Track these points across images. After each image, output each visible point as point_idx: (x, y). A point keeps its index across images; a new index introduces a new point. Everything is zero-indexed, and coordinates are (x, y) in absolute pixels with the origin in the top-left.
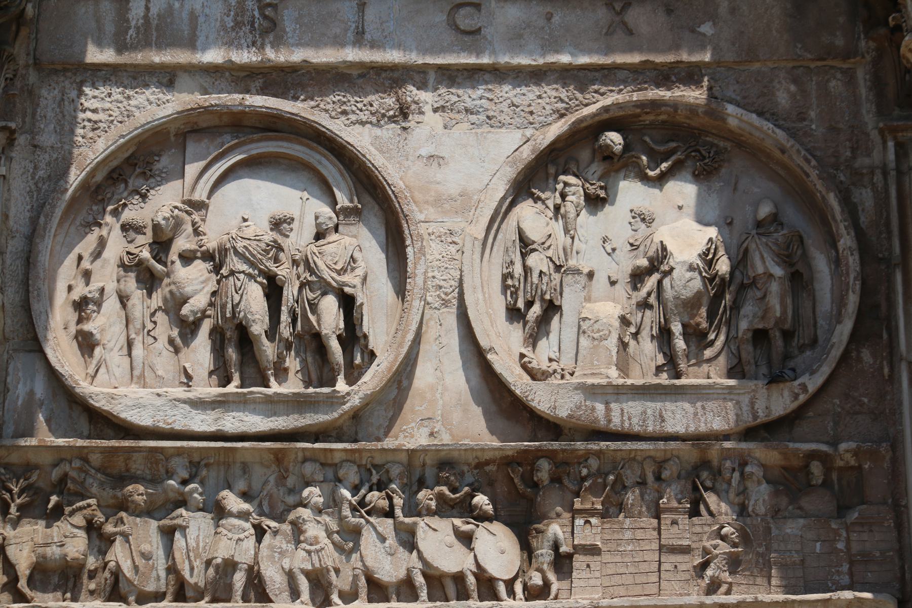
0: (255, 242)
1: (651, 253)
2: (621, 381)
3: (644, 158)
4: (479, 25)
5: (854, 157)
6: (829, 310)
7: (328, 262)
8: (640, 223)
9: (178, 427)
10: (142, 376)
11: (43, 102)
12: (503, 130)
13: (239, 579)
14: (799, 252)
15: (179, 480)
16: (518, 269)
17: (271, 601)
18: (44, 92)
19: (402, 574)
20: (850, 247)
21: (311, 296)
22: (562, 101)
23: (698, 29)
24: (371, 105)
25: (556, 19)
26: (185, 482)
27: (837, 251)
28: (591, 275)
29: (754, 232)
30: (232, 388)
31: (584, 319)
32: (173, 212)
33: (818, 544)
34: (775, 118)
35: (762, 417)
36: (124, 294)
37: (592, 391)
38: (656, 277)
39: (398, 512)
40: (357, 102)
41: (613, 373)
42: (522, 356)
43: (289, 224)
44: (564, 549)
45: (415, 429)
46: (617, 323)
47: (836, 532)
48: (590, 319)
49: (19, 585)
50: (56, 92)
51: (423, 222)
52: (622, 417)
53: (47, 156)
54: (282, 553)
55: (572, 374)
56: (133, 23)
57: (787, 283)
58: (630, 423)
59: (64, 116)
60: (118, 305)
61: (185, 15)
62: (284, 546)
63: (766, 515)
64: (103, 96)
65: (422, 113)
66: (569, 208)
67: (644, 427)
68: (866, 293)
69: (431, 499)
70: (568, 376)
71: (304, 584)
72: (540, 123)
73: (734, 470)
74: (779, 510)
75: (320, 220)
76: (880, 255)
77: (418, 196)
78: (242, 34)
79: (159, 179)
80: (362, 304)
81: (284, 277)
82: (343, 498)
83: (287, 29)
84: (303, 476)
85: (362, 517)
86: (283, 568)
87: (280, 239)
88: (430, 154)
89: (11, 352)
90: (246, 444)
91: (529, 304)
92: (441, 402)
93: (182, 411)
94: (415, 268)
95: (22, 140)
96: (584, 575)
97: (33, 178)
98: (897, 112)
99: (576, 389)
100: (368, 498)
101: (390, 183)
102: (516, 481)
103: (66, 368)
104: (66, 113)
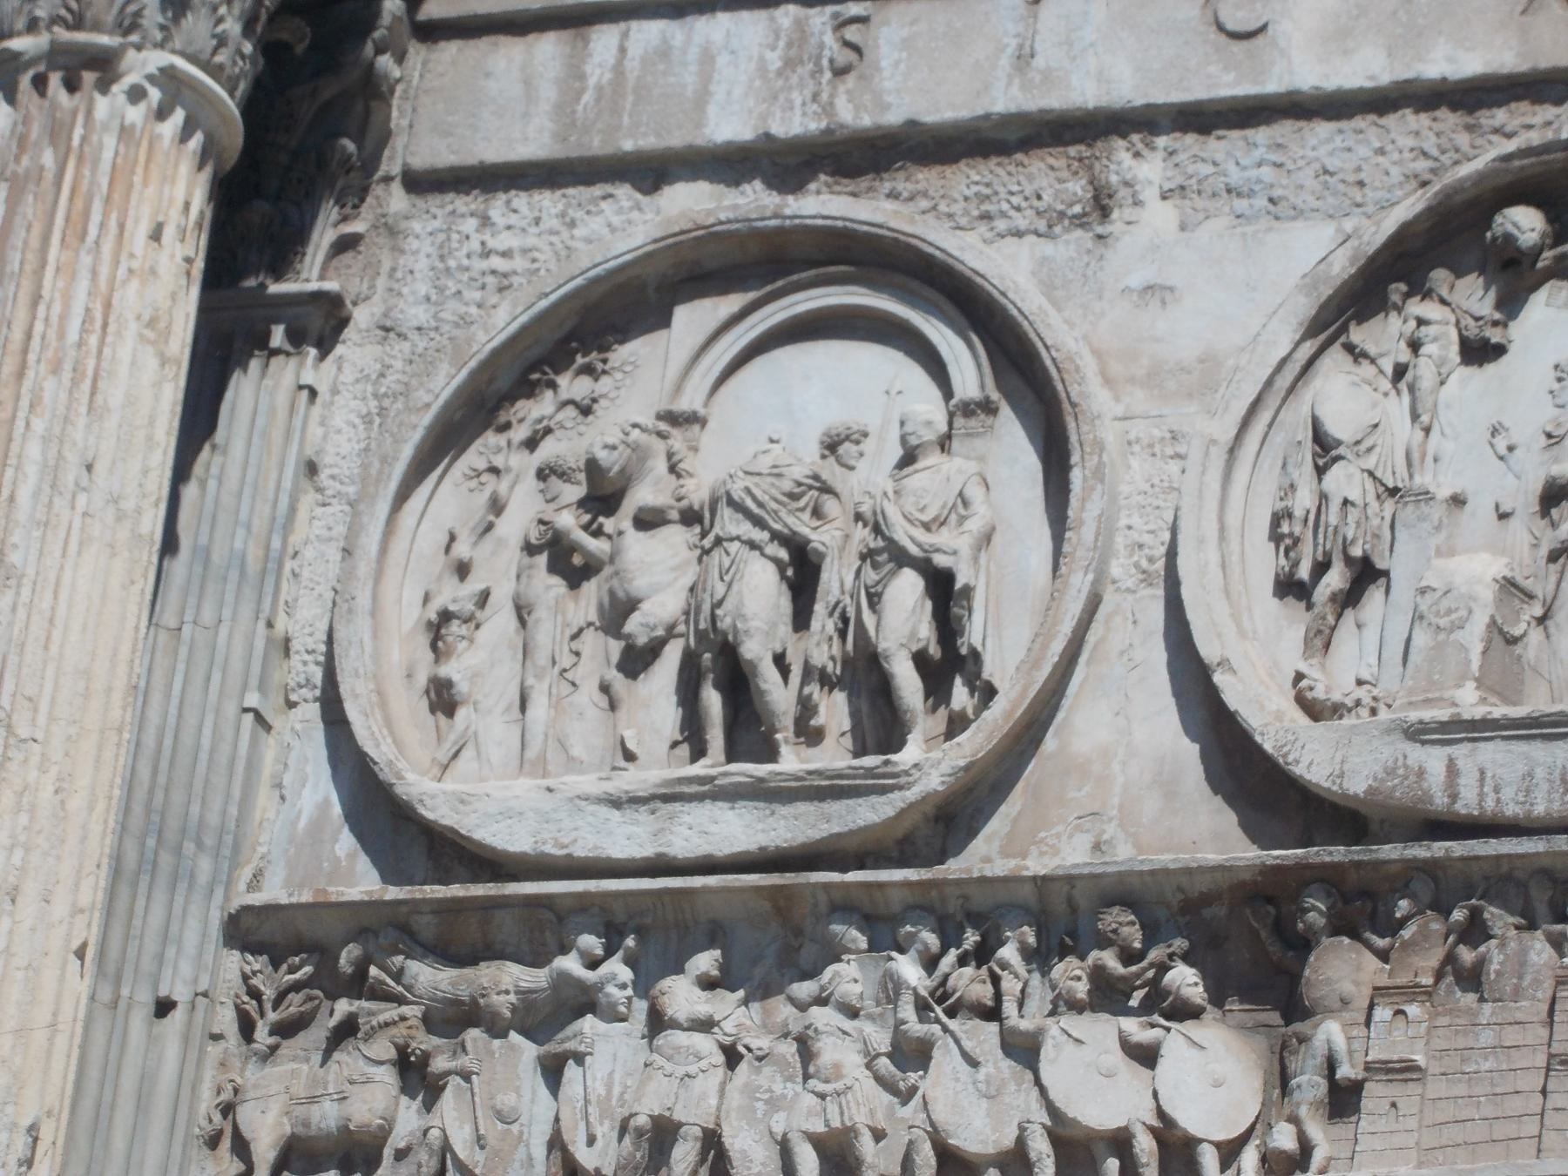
0: (770, 479)
9: (580, 851)
10: (542, 759)
12: (1299, 224)
19: (1008, 1140)
22: (1425, 154)
24: (1039, 197)
26: (593, 964)
28: (1458, 501)
31: (1423, 591)
32: (627, 434)
36: (522, 603)
37: (1417, 733)
39: (1009, 1008)
40: (1012, 193)
42: (1299, 677)
43: (858, 442)
44: (1345, 1071)
45: (1064, 838)
48: (1434, 590)
51: (1120, 419)
52: (1482, 786)
53: (406, 346)
54: (774, 1104)
58: (1498, 801)
60: (513, 623)
61: (693, 53)
62: (778, 1088)
64: (524, 223)
65: (1137, 203)
67: (1527, 806)
69: (1079, 979)
72: (1377, 203)
77: (1116, 368)
78: (794, 79)
79: (619, 376)
81: (823, 544)
83: (884, 63)
85: (938, 1021)
86: (771, 1133)
88: (1145, 284)
91: (1321, 568)
93: (590, 819)
94: (1082, 508)
95: (362, 317)
96: (1381, 1125)
99: (1388, 731)
101: (1049, 343)
102: (1263, 934)
103: (384, 748)
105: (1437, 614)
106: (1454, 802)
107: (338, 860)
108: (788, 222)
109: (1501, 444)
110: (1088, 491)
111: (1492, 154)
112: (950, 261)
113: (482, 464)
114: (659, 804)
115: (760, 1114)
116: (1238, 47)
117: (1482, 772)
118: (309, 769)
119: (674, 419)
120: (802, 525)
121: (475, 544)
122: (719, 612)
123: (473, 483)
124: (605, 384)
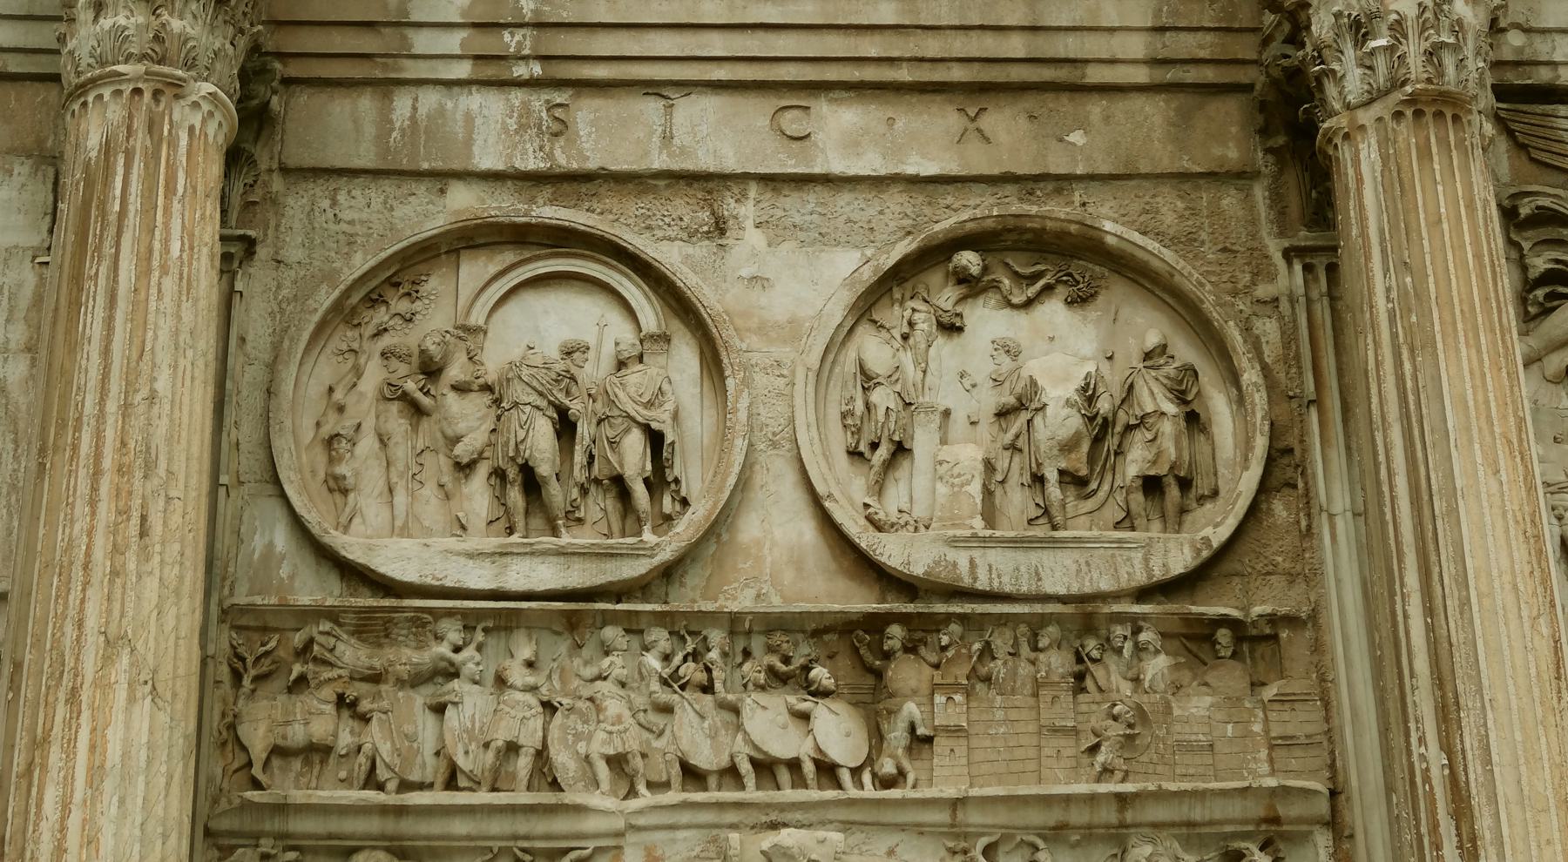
1: (1018, 390)
2: (988, 533)
3: (1007, 282)
7: (632, 394)
8: (1004, 355)
9: (449, 583)
12: (839, 249)
13: (523, 764)
16: (859, 406)
17: (563, 791)
18: (290, 201)
19: (724, 761)
21: (610, 433)
24: (681, 219)
25: (899, 124)
26: (457, 650)
27: (1239, 388)
29: (1141, 365)
30: (515, 538)
35: (1158, 574)
36: (383, 431)
37: (954, 542)
38: (1024, 416)
39: (718, 686)
41: (978, 523)
42: (867, 506)
44: (921, 731)
46: (981, 467)
47: (1251, 712)
49: (253, 771)
50: (304, 201)
53: (293, 272)
54: (578, 737)
55: (927, 528)
56: (398, 125)
57: (1183, 424)
60: (377, 445)
61: (459, 116)
63: (1166, 692)
66: (918, 337)
68: (1274, 433)
70: (922, 529)
71: (603, 770)
73: (1125, 638)
75: (622, 347)
76: (1291, 394)
77: (739, 322)
79: (427, 302)
80: (673, 443)
82: (652, 671)
83: (582, 133)
84: (602, 643)
85: (676, 692)
87: (574, 370)
90: (534, 605)
91: (874, 446)
92: (769, 559)
94: (737, 401)
95: (262, 252)
96: (947, 761)
97: (275, 299)
98: (1303, 233)
99: (934, 541)
100: (681, 672)
102: (862, 652)
104: (316, 225)
107: (282, 579)
108: (534, 221)
109: (966, 381)
110: (739, 393)
111: (952, 221)
114: (497, 558)
116: (795, 145)
117: (990, 566)
118: (257, 523)
119: (468, 329)
122: (522, 447)
123: (340, 359)
124: (418, 306)
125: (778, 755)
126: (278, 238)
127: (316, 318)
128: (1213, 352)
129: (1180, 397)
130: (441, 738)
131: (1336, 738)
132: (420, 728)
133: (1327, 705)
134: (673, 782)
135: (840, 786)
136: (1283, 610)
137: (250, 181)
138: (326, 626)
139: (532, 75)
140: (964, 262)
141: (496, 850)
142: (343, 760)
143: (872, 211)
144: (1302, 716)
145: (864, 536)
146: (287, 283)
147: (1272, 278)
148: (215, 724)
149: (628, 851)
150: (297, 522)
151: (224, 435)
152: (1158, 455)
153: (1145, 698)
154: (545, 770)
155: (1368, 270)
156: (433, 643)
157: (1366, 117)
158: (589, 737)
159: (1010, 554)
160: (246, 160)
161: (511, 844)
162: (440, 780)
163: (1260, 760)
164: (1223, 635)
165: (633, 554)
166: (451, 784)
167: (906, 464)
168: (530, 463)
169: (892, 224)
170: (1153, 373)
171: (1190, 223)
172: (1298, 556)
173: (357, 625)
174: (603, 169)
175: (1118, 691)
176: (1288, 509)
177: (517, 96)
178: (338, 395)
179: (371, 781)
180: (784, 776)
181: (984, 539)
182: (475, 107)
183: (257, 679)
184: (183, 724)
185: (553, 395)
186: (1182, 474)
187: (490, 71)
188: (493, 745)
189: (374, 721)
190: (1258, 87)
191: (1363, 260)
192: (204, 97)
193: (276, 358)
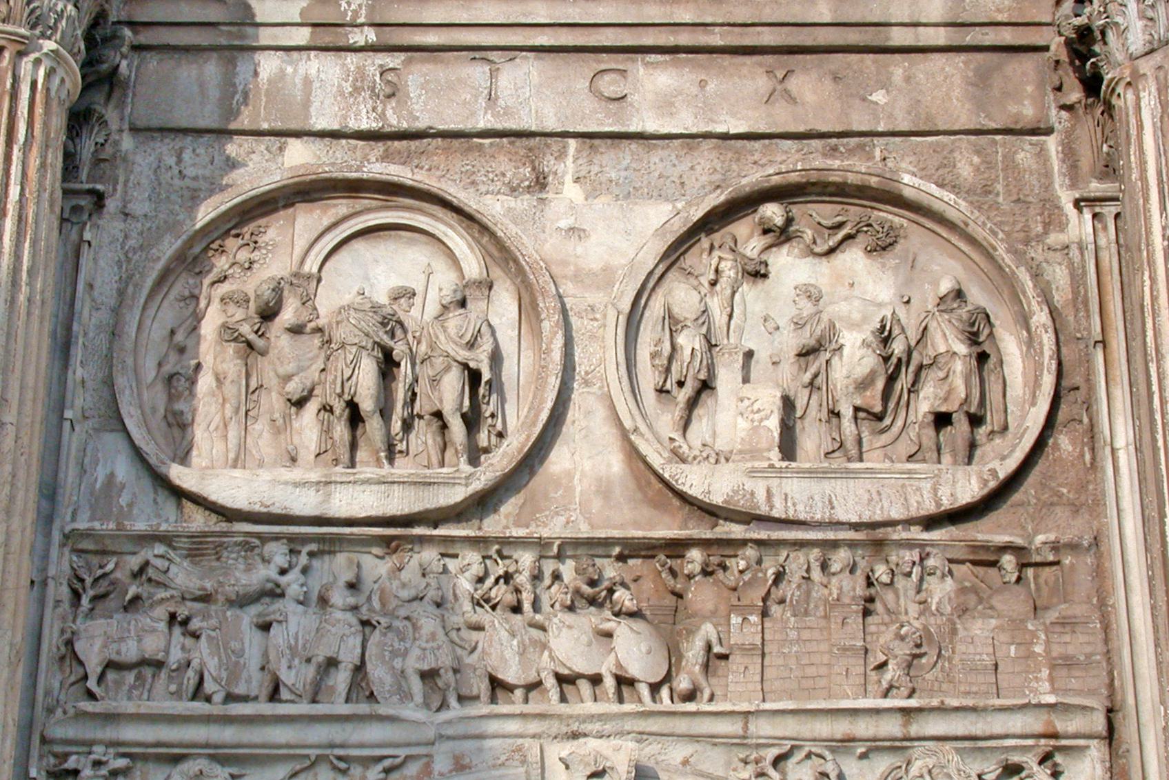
4: (625, 92)
5: (1046, 233)
6: (1021, 395)
8: (806, 300)
9: (276, 510)
11: (137, 169)
12: (650, 202)
13: (341, 679)
14: (986, 332)
15: (277, 570)
18: (139, 159)
20: (1044, 325)
23: (870, 98)
25: (711, 87)
26: (283, 572)
27: (1028, 331)
29: (936, 309)
33: (1013, 648)
34: (957, 190)
35: (947, 504)
39: (527, 606)
40: (488, 172)
41: (775, 455)
44: (717, 649)
46: (779, 403)
47: (1034, 634)
50: (152, 159)
53: (139, 225)
54: (395, 654)
55: (727, 460)
56: (240, 88)
59: (160, 184)
63: (952, 614)
66: (724, 283)
70: (723, 460)
71: (416, 685)
73: (914, 563)
74: (967, 609)
76: (1079, 335)
77: (555, 270)
79: (264, 252)
89: (90, 431)
90: (355, 530)
91: (681, 384)
92: (578, 489)
94: (551, 342)
95: (111, 205)
97: (122, 248)
105: (752, 411)
106: (771, 510)
107: (122, 507)
108: (365, 176)
109: (771, 325)
111: (758, 175)
112: (462, 205)
113: (187, 293)
115: (387, 658)
116: (613, 106)
117: (786, 495)
120: (386, 339)
121: (186, 338)
123: (182, 304)
124: (256, 255)
125: (581, 672)
126: (126, 192)
127: (160, 265)
128: (1005, 297)
129: (973, 338)
130: (265, 654)
131: (1115, 659)
132: (247, 645)
133: (1106, 628)
134: (482, 695)
135: (640, 701)
136: (1065, 539)
137: (101, 140)
138: (160, 549)
139: (367, 41)
140: (769, 213)
141: (313, 758)
142: (174, 674)
143: (684, 167)
144: (1082, 638)
145: (668, 467)
146: (134, 235)
147: (1062, 227)
148: (54, 641)
149: (437, 759)
150: (138, 454)
151: (70, 372)
152: (949, 392)
153: (932, 620)
154: (363, 684)
155: (1147, 210)
156: (261, 566)
157: (1146, 66)
158: (405, 654)
159: (805, 483)
160: (97, 121)
161: (328, 752)
162: (265, 692)
163: (1041, 680)
164: (1008, 561)
165: (449, 483)
166: (274, 696)
167: (710, 402)
168: (356, 400)
169: (704, 179)
170: (946, 316)
171: (986, 175)
172: (1082, 487)
173: (190, 549)
174: (431, 128)
175: (906, 613)
176: (1074, 444)
177: (352, 59)
178: (179, 337)
179: (198, 692)
180: (584, 686)
181: (780, 470)
182: (313, 72)
183: (96, 599)
184: (9, 633)
185: (378, 336)
186: (973, 410)
187: (327, 38)
188: (314, 660)
189: (203, 638)
190: (1053, 48)
191: (1141, 201)
192: (46, 54)
193: (121, 303)
